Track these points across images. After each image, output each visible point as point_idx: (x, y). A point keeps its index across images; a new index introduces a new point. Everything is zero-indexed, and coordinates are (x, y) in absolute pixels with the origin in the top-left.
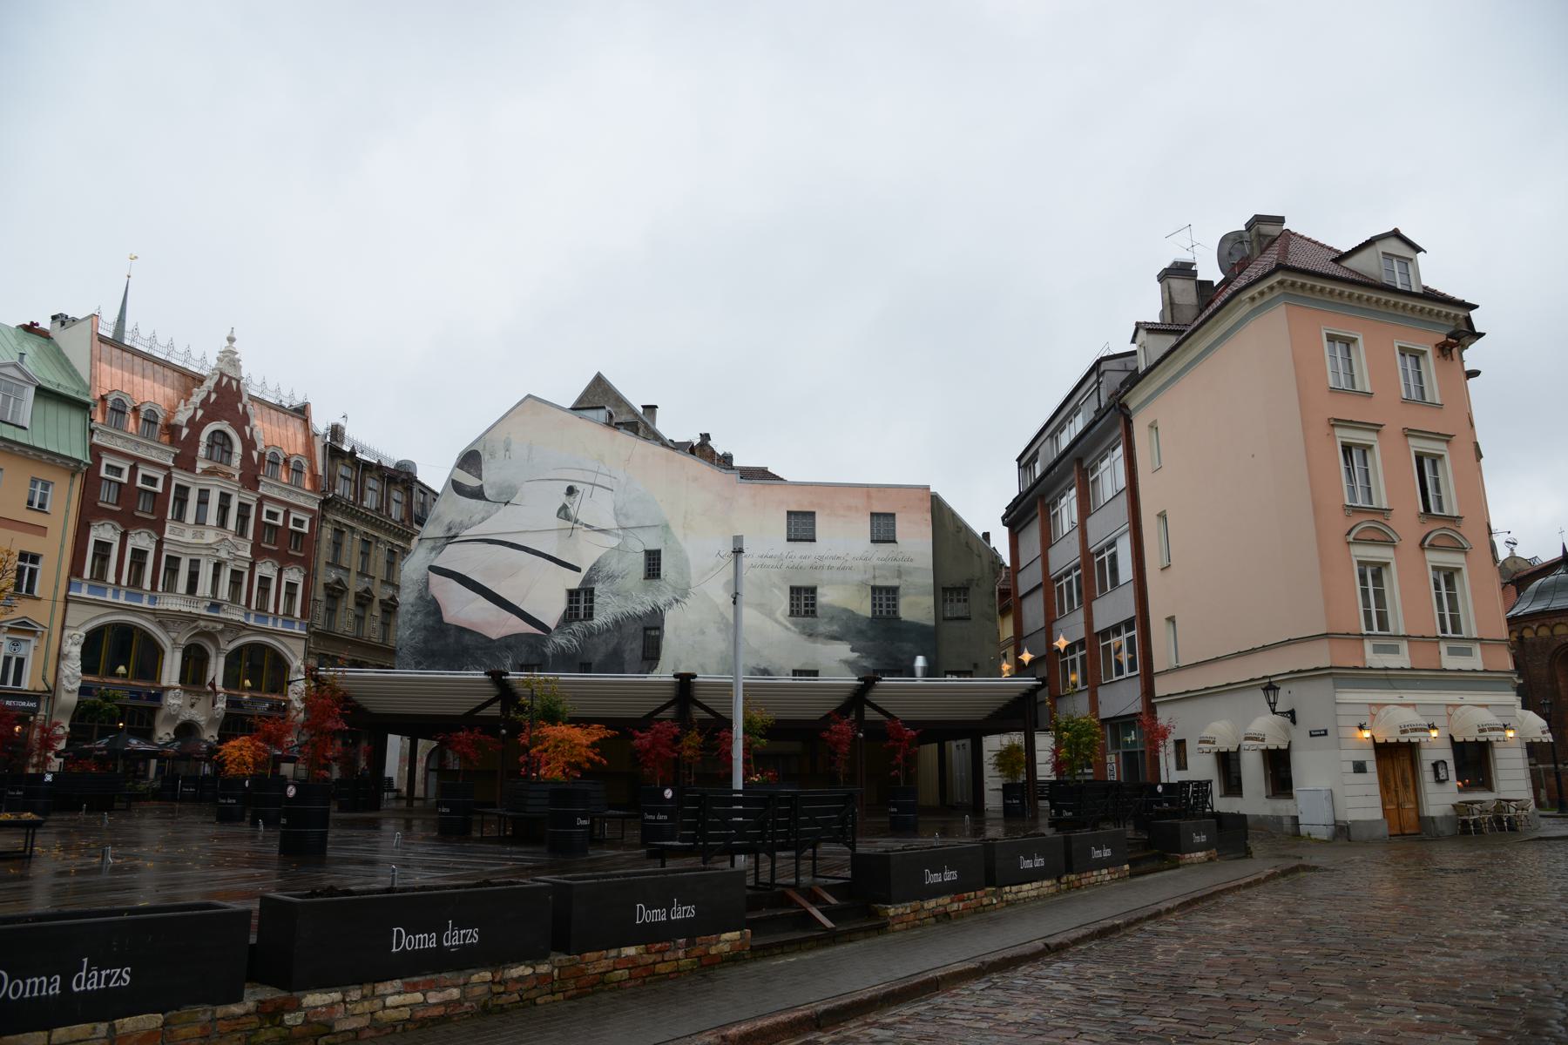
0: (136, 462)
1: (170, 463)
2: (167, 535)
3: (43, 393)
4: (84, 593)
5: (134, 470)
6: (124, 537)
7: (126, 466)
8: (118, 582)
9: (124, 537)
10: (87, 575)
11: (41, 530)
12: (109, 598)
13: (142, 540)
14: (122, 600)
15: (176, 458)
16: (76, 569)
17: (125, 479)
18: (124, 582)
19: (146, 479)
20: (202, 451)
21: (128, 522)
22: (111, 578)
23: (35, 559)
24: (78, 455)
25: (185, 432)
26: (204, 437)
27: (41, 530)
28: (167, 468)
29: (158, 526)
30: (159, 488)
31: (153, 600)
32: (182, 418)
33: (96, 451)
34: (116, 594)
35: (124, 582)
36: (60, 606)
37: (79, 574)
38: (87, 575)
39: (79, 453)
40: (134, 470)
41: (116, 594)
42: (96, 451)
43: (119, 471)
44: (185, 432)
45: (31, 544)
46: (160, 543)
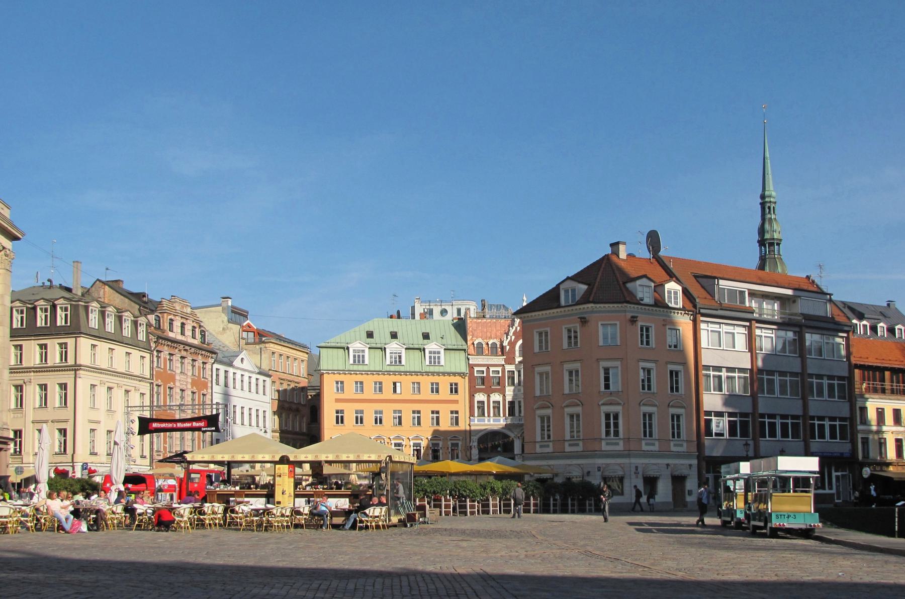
0: (488, 366)
6: (489, 396)
7: (484, 369)
8: (489, 416)
9: (489, 396)
11: (456, 402)
15: (505, 360)
16: (472, 414)
18: (492, 415)
20: (517, 353)
21: (488, 392)
22: (486, 415)
23: (457, 412)
25: (508, 348)
26: (517, 348)
27: (456, 402)
33: (471, 367)
35: (492, 415)
37: (473, 416)
39: (464, 369)
42: (471, 367)
44: (508, 348)
45: (454, 407)
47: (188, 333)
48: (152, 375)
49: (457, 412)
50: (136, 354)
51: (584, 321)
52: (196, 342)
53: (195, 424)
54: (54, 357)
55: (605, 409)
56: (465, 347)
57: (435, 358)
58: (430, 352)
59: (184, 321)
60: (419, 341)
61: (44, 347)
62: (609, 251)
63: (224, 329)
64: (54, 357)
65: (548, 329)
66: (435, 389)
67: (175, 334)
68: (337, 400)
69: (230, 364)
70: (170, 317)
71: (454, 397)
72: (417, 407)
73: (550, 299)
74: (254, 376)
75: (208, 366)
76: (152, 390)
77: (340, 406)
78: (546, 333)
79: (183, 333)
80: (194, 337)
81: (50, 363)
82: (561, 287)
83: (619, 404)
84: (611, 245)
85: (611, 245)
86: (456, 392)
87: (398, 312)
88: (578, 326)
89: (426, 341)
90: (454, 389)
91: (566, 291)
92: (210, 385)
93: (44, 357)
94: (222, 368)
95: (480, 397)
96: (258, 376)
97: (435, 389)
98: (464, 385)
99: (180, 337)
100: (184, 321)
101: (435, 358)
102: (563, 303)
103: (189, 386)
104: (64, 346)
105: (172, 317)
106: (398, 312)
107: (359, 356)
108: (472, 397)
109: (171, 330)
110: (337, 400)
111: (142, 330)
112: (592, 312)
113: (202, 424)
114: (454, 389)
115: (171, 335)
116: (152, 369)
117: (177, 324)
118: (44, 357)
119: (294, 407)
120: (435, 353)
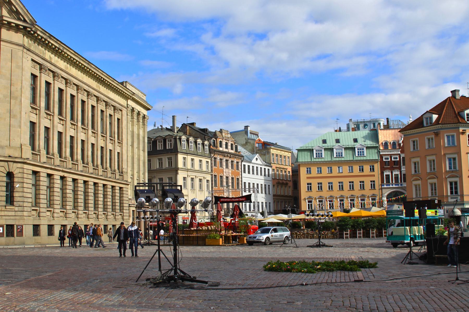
0: (391, 155)
1: (399, 153)
2: (402, 169)
3: (367, 148)
4: (385, 186)
5: (391, 157)
6: (392, 173)
9: (392, 173)
10: (385, 182)
11: (374, 176)
12: (391, 186)
13: (396, 172)
14: (394, 186)
16: (382, 181)
17: (389, 160)
18: (394, 182)
19: (394, 158)
21: (392, 169)
23: (374, 181)
24: (377, 158)
25: (402, 144)
27: (374, 176)
28: (399, 154)
29: (400, 169)
30: (398, 160)
31: (401, 185)
32: (401, 142)
33: (381, 157)
34: (392, 185)
35: (394, 182)
36: (381, 191)
38: (385, 182)
40: (391, 157)
41: (392, 185)
42: (381, 157)
43: (388, 159)
44: (402, 144)
45: (372, 179)
46: (401, 172)
47: (229, 147)
48: (212, 170)
49: (374, 181)
50: (204, 160)
51: (437, 134)
52: (233, 152)
53: (240, 199)
54: (166, 165)
55: (449, 180)
56: (377, 145)
57: (361, 152)
58: (358, 149)
59: (227, 141)
60: (351, 143)
61: (160, 160)
62: (450, 95)
63: (246, 143)
64: (166, 165)
65: (418, 139)
66: (362, 170)
67: (223, 149)
68: (308, 178)
69: (251, 162)
70: (220, 140)
71: (372, 173)
72: (351, 179)
73: (418, 123)
74: (263, 167)
75: (240, 164)
76: (212, 178)
77: (309, 181)
78: (417, 141)
79: (227, 147)
80: (232, 149)
81: (164, 167)
82: (424, 116)
83: (457, 177)
84: (451, 92)
85: (451, 92)
86: (373, 170)
87: (340, 128)
88: (433, 136)
89: (355, 143)
90: (372, 169)
91: (427, 118)
92: (240, 173)
93: (161, 164)
94: (247, 164)
95: (386, 173)
96: (265, 167)
97: (362, 170)
98: (377, 167)
99: (225, 150)
100: (227, 141)
101: (361, 152)
102: (425, 124)
103: (230, 175)
104: (170, 159)
105: (221, 140)
106: (340, 128)
107: (319, 153)
108: (382, 173)
109: (221, 146)
110: (308, 178)
111: (207, 148)
112: (441, 129)
113: (244, 199)
114: (372, 169)
115: (221, 149)
116: (212, 167)
117: (224, 143)
118: (161, 164)
119: (284, 182)
120: (361, 149)
